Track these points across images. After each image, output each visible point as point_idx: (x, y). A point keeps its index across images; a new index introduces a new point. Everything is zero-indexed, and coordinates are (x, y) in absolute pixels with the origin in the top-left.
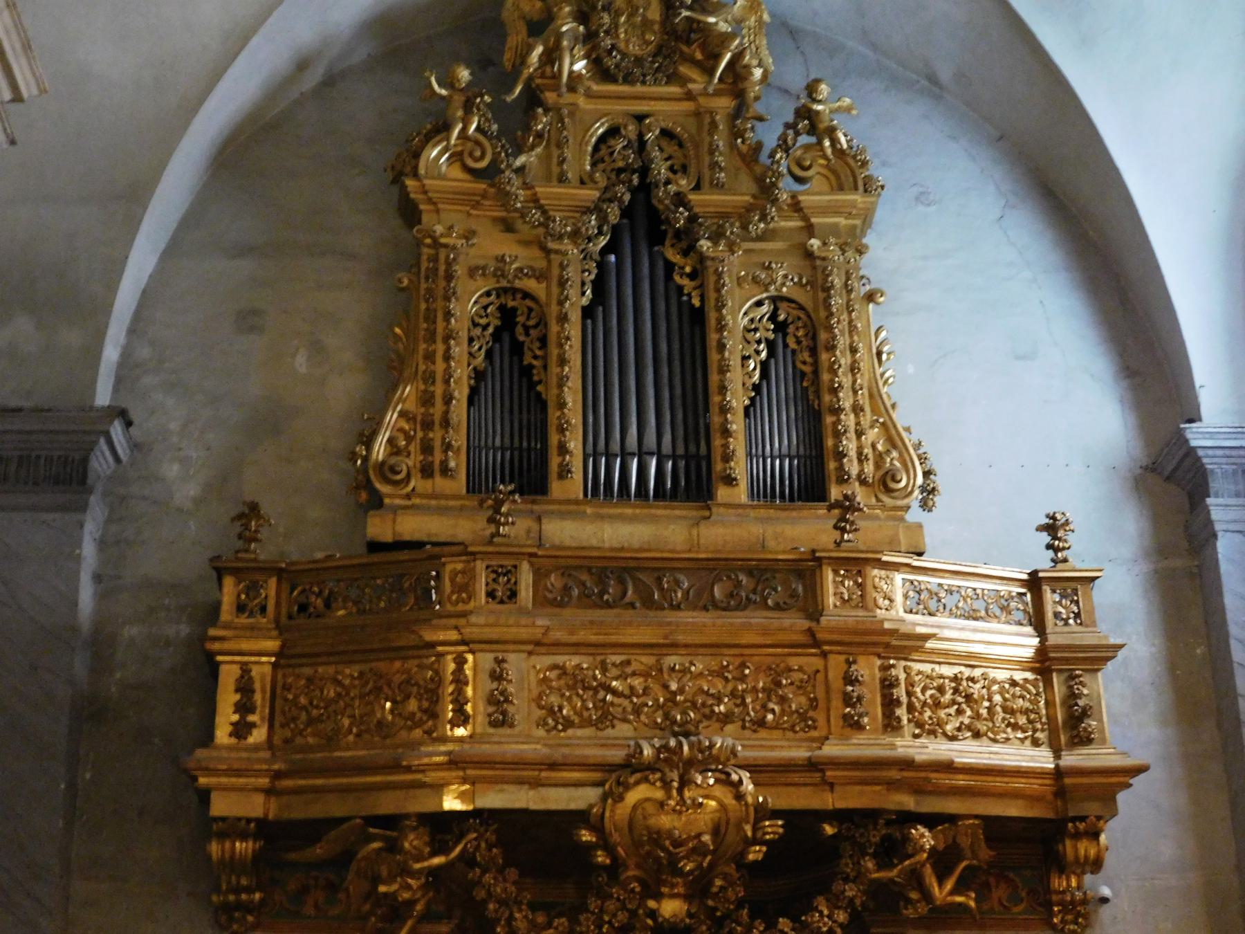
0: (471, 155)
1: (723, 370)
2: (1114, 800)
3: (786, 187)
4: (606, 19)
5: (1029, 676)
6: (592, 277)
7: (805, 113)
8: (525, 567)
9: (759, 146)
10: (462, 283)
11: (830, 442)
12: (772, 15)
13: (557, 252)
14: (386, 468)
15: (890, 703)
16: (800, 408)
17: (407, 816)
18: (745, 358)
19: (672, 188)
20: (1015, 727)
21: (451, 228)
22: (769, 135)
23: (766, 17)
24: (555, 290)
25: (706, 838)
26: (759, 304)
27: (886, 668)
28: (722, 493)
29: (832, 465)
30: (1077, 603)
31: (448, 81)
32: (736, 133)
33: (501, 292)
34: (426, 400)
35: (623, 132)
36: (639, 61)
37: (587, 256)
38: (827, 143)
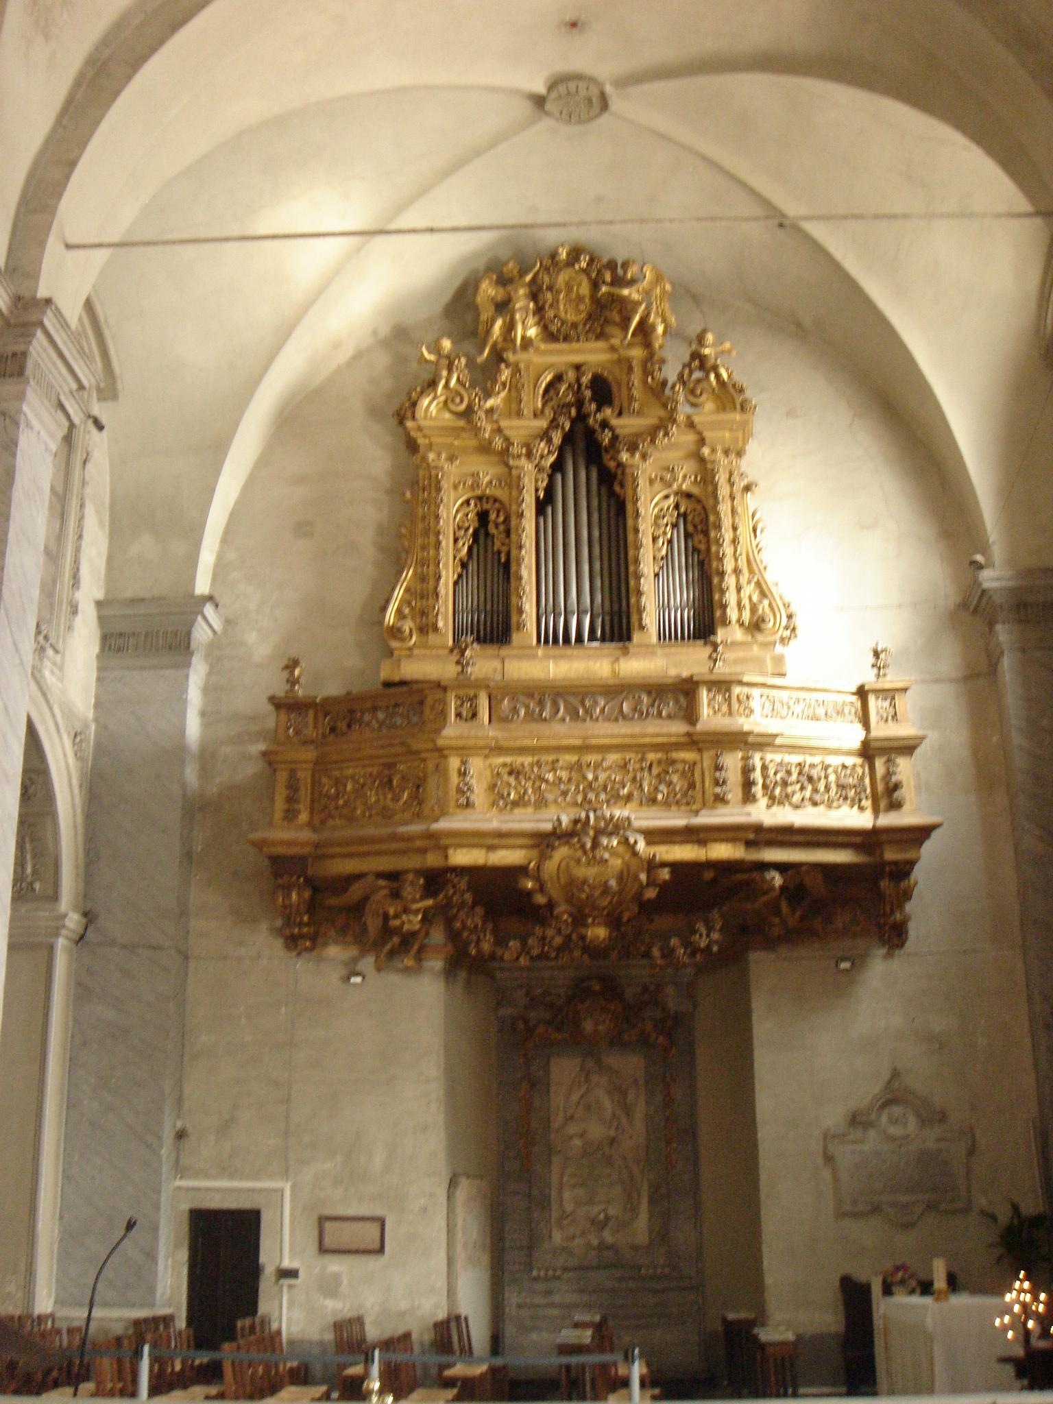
1: (638, 547)
3: (683, 411)
5: (859, 761)
6: (545, 484)
7: (696, 355)
9: (664, 383)
11: (717, 597)
12: (673, 284)
13: (517, 467)
14: (395, 631)
16: (696, 574)
17: (405, 872)
19: (599, 416)
21: (439, 455)
23: (668, 287)
24: (514, 493)
26: (667, 497)
27: (746, 759)
28: (637, 637)
29: (718, 613)
31: (436, 349)
32: (647, 372)
34: (423, 578)
36: (574, 326)
37: (540, 469)
38: (712, 376)
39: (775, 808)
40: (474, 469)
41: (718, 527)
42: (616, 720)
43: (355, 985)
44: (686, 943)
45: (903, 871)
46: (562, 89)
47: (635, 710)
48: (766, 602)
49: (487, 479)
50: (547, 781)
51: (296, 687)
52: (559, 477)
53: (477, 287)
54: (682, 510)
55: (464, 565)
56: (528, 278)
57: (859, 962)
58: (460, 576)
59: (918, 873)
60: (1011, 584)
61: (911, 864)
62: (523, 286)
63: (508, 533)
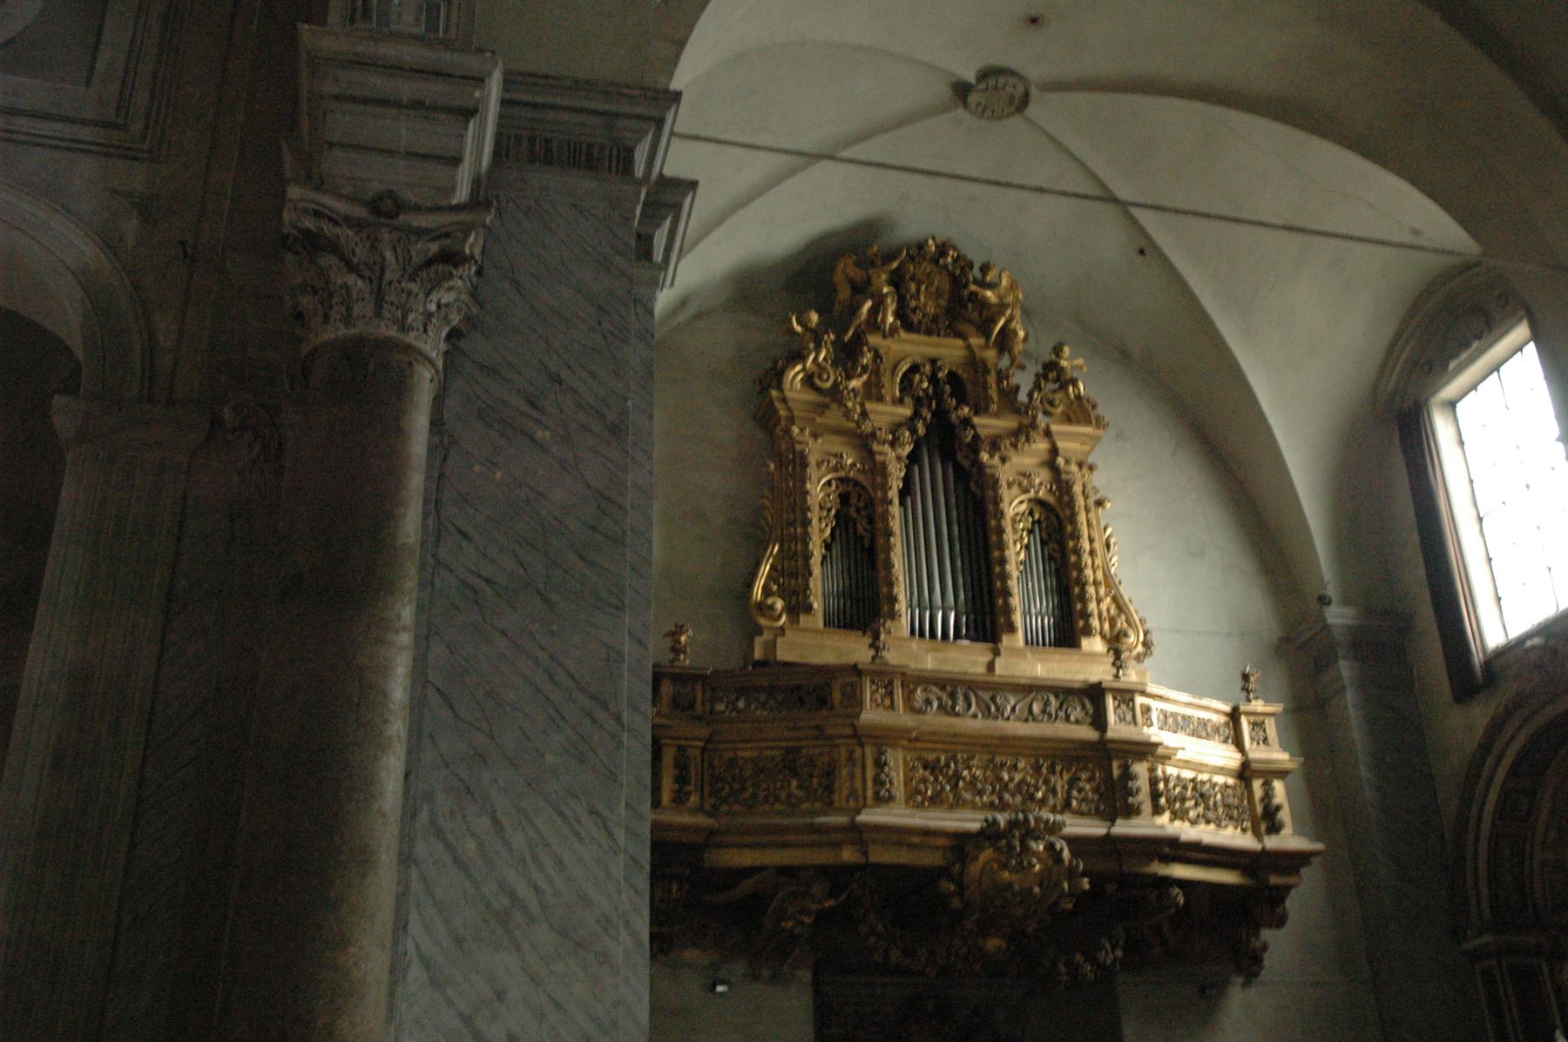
0: (820, 377)
2: (1299, 870)
3: (1042, 420)
4: (913, 286)
8: (897, 683)
10: (812, 471)
13: (880, 453)
15: (1155, 795)
16: (1054, 583)
18: (1015, 542)
20: (1231, 818)
21: (802, 430)
22: (1023, 381)
25: (1037, 890)
26: (1021, 502)
27: (1152, 770)
28: (1006, 640)
30: (1264, 731)
33: (841, 480)
35: (922, 370)
36: (935, 319)
37: (899, 458)
39: (1177, 823)
40: (837, 449)
41: (1076, 536)
42: (1026, 720)
43: (721, 994)
44: (1091, 959)
45: (1279, 895)
46: (991, 82)
47: (1044, 711)
48: (1123, 617)
49: (850, 461)
50: (964, 779)
51: (682, 657)
52: (916, 469)
53: (833, 269)
54: (1037, 517)
55: (828, 547)
56: (895, 265)
57: (1221, 987)
58: (824, 557)
59: (1292, 903)
60: (1351, 622)
61: (1288, 888)
62: (884, 272)
63: (871, 520)
